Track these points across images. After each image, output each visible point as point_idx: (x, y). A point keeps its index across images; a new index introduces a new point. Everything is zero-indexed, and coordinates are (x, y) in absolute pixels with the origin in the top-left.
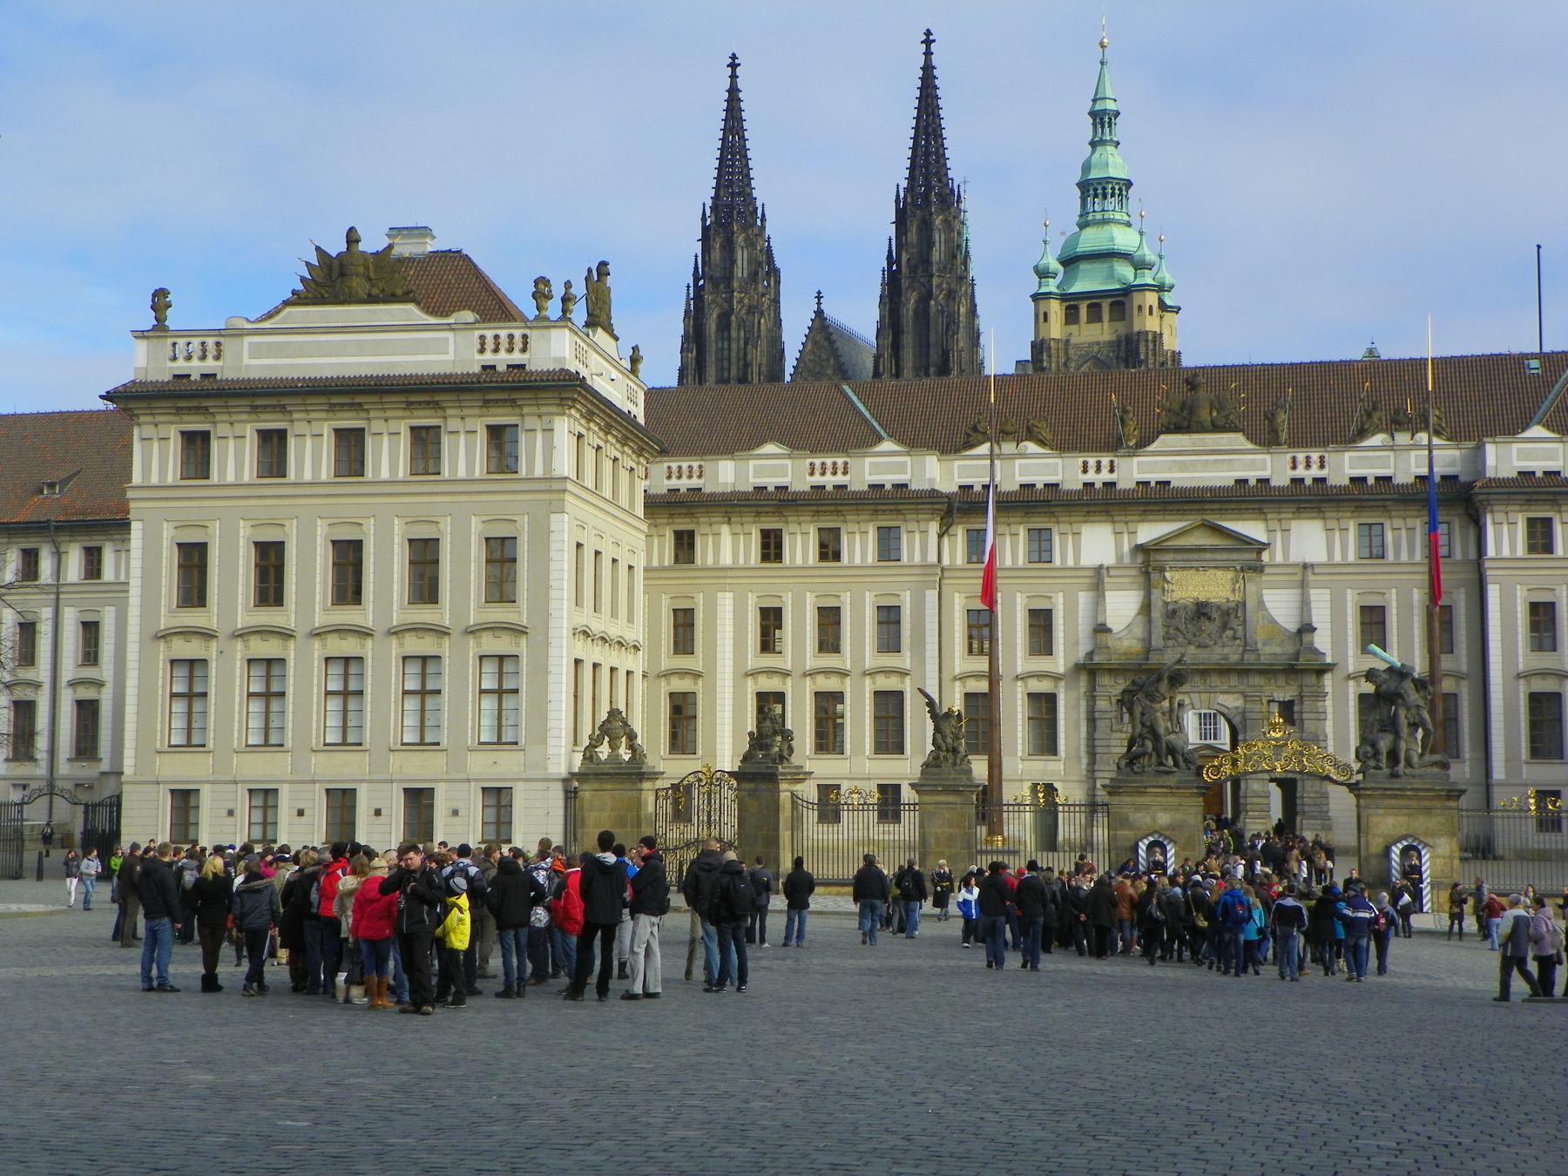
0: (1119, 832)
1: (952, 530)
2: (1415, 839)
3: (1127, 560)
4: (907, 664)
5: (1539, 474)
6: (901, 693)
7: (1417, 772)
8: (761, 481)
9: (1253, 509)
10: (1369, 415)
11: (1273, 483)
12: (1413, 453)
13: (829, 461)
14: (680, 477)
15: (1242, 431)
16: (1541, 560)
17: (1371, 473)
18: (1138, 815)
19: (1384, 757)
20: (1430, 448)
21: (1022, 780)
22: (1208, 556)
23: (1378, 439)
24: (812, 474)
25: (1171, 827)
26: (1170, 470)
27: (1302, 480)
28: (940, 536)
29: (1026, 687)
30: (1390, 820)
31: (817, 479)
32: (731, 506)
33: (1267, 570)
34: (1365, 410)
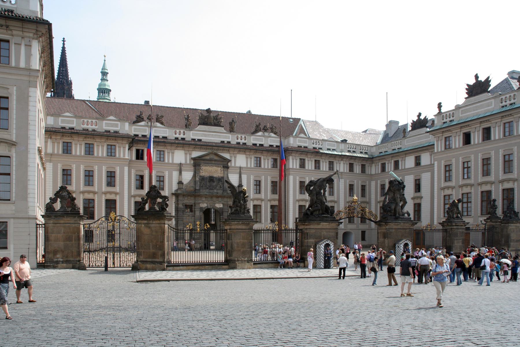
0: (309, 240)
1: (131, 149)
3: (188, 162)
4: (118, 191)
5: (303, 147)
9: (226, 150)
11: (231, 143)
12: (269, 139)
15: (223, 127)
16: (302, 170)
17: (258, 143)
19: (393, 212)
22: (213, 162)
23: (260, 133)
26: (202, 136)
27: (239, 143)
28: (128, 150)
33: (230, 168)
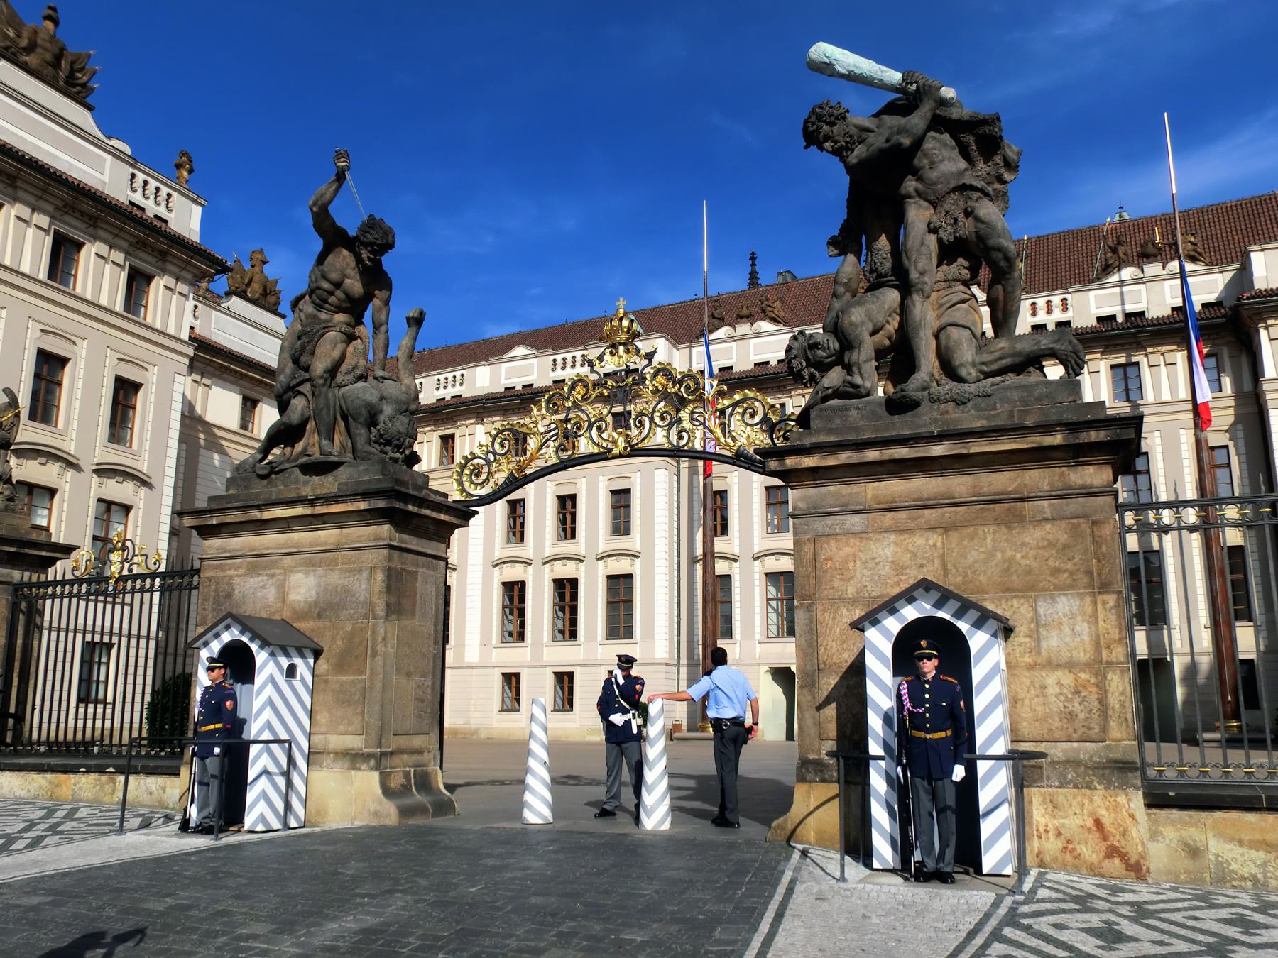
2: (964, 608)
6: (630, 577)
7: (971, 388)
8: (509, 383)
10: (1114, 251)
13: (569, 356)
14: (445, 387)
18: (253, 582)
20: (1183, 275)
21: (759, 664)
23: (1128, 273)
24: (554, 369)
25: (323, 609)
27: (1043, 326)
29: (763, 566)
30: (886, 549)
31: (559, 374)
32: (480, 407)
34: (1110, 247)
